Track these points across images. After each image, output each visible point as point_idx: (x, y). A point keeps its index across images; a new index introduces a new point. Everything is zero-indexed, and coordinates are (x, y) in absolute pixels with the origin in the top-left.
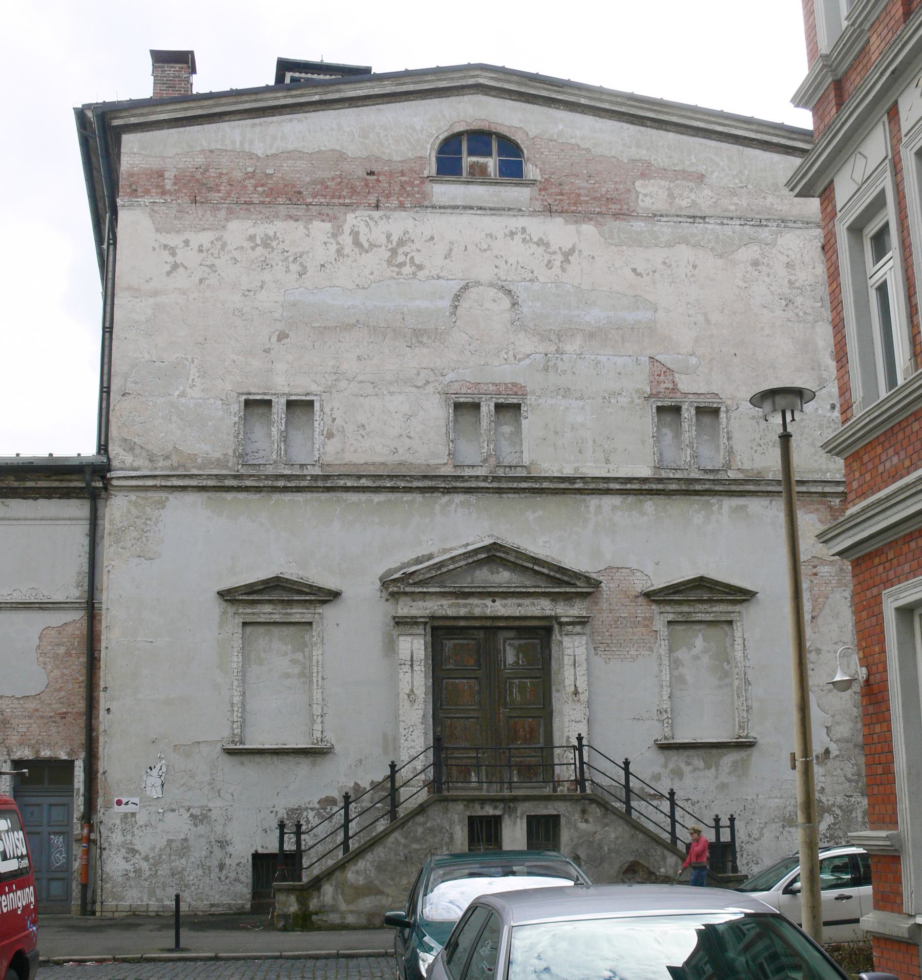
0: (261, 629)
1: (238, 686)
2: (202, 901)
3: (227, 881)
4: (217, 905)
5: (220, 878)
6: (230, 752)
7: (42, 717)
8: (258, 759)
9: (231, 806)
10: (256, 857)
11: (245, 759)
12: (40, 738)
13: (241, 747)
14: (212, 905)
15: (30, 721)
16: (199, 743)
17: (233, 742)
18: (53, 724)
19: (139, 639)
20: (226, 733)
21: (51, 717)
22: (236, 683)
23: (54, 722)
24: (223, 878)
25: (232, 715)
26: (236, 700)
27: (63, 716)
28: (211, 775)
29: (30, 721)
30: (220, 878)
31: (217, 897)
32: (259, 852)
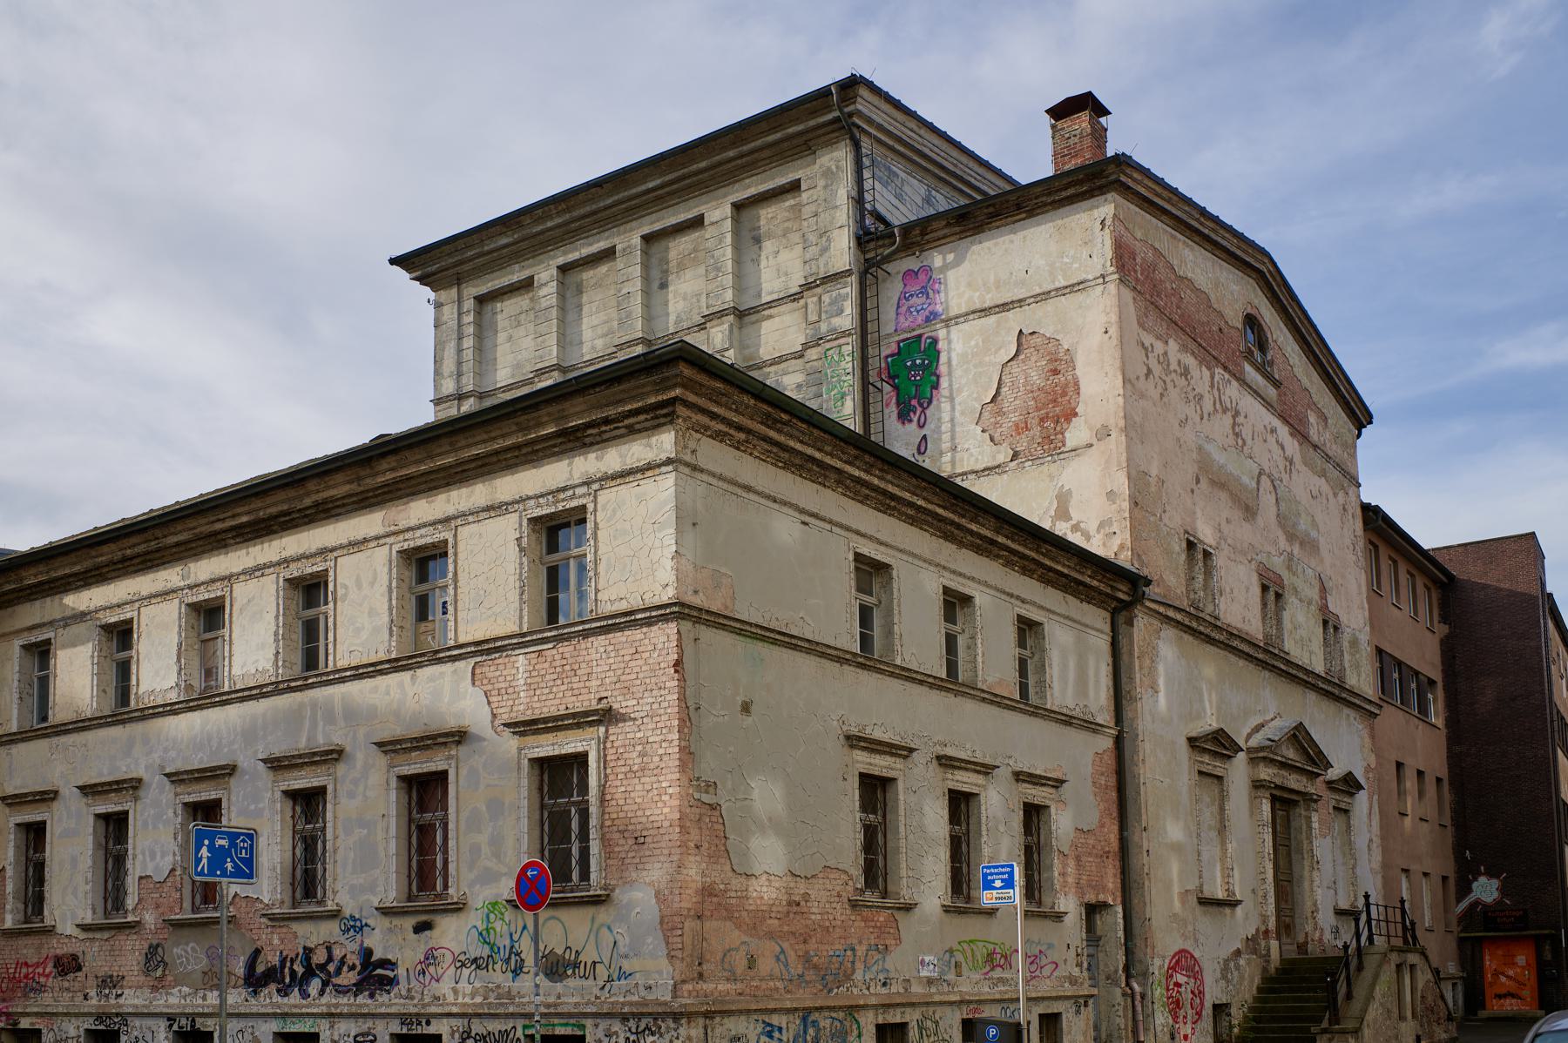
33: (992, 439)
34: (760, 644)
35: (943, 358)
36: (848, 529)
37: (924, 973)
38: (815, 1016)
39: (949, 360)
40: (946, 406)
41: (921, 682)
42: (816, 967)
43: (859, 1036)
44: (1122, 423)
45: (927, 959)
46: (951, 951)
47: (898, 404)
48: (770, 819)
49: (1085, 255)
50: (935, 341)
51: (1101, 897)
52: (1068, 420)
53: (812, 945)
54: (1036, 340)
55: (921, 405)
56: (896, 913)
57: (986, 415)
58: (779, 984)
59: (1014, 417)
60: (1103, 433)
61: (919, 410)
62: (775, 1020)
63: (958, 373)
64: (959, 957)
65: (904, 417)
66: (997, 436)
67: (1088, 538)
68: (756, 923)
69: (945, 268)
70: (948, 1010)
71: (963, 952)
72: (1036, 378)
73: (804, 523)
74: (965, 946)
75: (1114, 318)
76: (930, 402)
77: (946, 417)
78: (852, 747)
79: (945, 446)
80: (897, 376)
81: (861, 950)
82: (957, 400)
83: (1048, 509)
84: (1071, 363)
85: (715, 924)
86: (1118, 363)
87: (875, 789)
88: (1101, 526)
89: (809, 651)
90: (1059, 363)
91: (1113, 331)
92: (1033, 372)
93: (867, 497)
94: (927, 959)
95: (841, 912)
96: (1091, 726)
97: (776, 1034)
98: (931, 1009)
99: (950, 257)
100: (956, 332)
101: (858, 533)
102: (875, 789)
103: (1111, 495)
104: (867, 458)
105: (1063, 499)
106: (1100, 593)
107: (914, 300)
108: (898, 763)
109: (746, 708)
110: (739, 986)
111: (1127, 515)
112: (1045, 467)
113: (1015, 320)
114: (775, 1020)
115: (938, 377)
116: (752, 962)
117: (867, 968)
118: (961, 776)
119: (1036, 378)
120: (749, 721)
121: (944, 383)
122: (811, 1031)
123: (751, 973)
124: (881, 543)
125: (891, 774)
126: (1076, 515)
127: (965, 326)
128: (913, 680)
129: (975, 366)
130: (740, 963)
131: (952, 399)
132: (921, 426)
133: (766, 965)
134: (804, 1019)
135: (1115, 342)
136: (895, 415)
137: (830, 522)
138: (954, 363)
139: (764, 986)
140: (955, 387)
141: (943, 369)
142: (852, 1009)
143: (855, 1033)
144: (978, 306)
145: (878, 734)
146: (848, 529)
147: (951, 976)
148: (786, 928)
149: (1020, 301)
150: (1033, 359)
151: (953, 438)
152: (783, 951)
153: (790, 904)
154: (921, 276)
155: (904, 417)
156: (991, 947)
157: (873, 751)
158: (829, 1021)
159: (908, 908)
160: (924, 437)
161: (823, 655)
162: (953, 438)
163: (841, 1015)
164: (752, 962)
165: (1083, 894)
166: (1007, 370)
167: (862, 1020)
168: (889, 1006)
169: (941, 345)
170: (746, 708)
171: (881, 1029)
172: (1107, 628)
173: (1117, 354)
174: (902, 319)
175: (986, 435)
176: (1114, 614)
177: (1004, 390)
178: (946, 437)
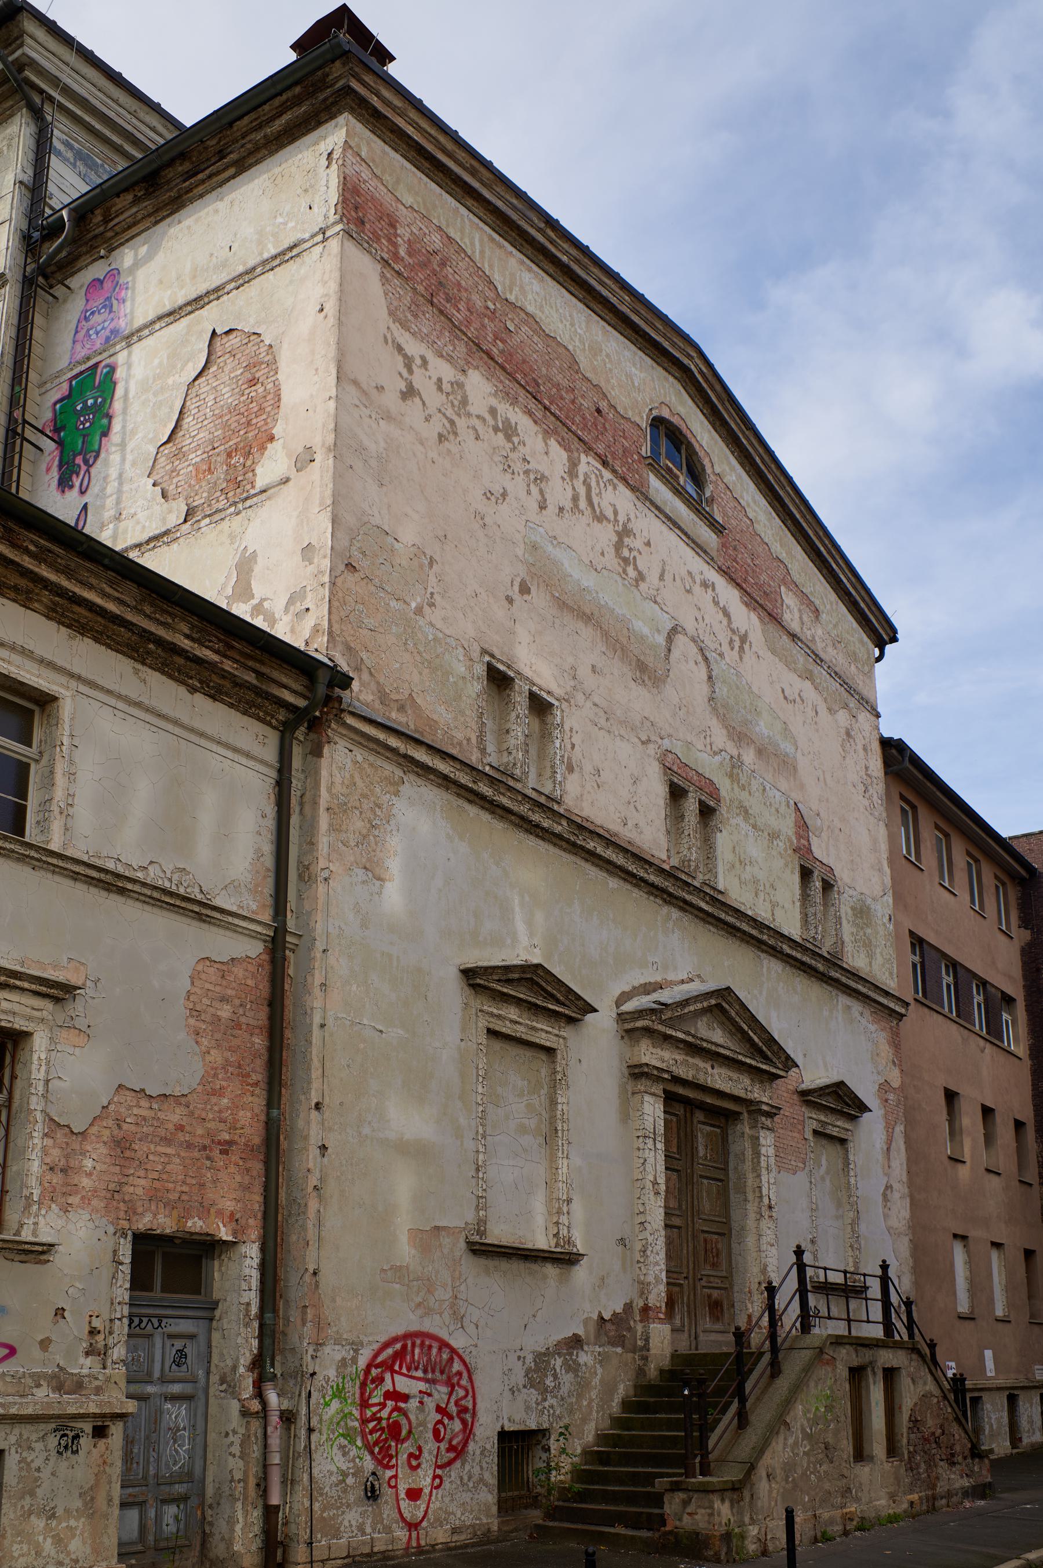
5: (461, 1478)
7: (189, 1146)
10: (504, 1436)
12: (185, 1188)
15: (169, 1151)
18: (208, 1163)
19: (365, 1022)
21: (205, 1148)
23: (208, 1158)
27: (226, 1147)
29: (169, 1151)
30: (461, 1478)
32: (506, 1429)
33: (164, 495)
35: (119, 392)
39: (126, 396)
40: (115, 458)
44: (330, 439)
47: (60, 466)
49: (304, 206)
50: (112, 369)
51: (195, 1224)
52: (263, 448)
54: (234, 340)
55: (86, 462)
57: (162, 460)
59: (195, 458)
60: (305, 459)
61: (84, 468)
63: (135, 407)
65: (64, 484)
66: (171, 489)
67: (273, 621)
69: (136, 265)
72: (228, 396)
75: (333, 286)
76: (97, 457)
77: (113, 473)
79: (108, 514)
80: (63, 428)
82: (129, 449)
83: (224, 586)
84: (273, 365)
86: (332, 352)
88: (291, 601)
90: (259, 369)
91: (331, 308)
92: (223, 389)
96: (201, 910)
99: (143, 250)
100: (139, 351)
103: (308, 552)
105: (245, 566)
106: (238, 684)
107: (97, 318)
111: (326, 579)
112: (225, 524)
113: (211, 317)
115: (110, 418)
119: (228, 396)
121: (117, 426)
126: (258, 590)
127: (149, 342)
129: (155, 395)
131: (123, 445)
132: (82, 493)
135: (331, 321)
136: (55, 482)
138: (131, 395)
140: (130, 426)
141: (117, 406)
144: (168, 307)
149: (217, 289)
150: (227, 369)
151: (118, 502)
154: (108, 285)
155: (64, 484)
160: (85, 507)
162: (118, 502)
166: (193, 392)
169: (120, 374)
172: (271, 754)
173: (333, 340)
174: (78, 347)
175: (158, 489)
176: (286, 732)
177: (188, 420)
178: (110, 502)
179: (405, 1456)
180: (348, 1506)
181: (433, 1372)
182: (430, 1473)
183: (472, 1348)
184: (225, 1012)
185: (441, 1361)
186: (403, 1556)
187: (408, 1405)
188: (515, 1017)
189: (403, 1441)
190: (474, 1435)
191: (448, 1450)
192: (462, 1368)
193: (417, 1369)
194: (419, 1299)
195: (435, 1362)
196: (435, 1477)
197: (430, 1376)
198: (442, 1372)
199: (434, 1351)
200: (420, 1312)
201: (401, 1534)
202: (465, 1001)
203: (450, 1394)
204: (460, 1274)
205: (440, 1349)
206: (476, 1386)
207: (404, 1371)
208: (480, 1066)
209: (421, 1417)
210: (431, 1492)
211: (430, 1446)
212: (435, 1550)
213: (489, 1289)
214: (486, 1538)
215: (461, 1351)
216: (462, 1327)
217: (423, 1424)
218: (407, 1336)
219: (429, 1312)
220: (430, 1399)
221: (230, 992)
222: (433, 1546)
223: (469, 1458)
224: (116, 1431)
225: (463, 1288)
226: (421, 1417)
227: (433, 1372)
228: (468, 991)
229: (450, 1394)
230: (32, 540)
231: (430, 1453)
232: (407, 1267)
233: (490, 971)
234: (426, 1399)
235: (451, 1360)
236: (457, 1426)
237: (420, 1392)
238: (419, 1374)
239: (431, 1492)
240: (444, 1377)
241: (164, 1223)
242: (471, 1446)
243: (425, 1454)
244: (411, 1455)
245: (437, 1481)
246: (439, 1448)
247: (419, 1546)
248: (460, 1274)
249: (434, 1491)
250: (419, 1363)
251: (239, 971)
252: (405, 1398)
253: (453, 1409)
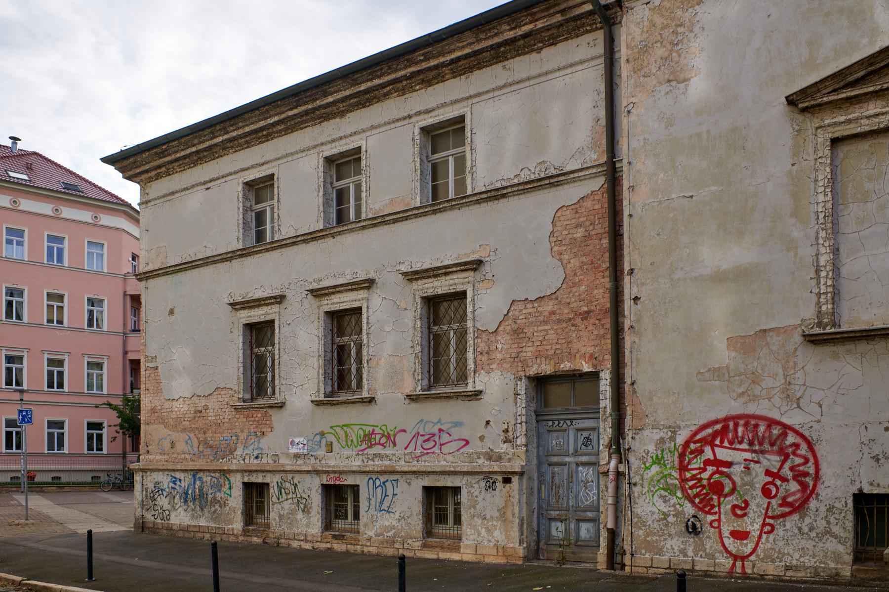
0: (864, 146)
1: (826, 238)
2: (773, 561)
3: (813, 534)
4: (797, 569)
5: (800, 529)
6: (813, 340)
7: (559, 321)
8: (863, 347)
9: (819, 421)
10: (860, 499)
11: (840, 349)
12: (558, 346)
13: (833, 330)
14: (788, 568)
15: (546, 327)
16: (765, 331)
17: (819, 324)
18: (573, 328)
19: (674, 196)
20: (809, 313)
21: (570, 320)
22: (822, 234)
23: (573, 325)
24: (806, 529)
25: (819, 283)
26: (823, 260)
27: (585, 316)
28: (785, 377)
29: (546, 327)
30: (800, 529)
31: (796, 556)
32: (865, 491)
34: (179, 274)
36: (236, 173)
37: (294, 450)
38: (200, 475)
41: (294, 244)
42: (211, 447)
43: (230, 488)
45: (296, 440)
46: (322, 434)
48: (184, 368)
53: (209, 435)
56: (269, 410)
58: (187, 456)
62: (178, 475)
64: (331, 438)
68: (177, 425)
70: (307, 478)
71: (336, 434)
73: (208, 189)
74: (338, 429)
78: (237, 310)
81: (242, 436)
85: (155, 426)
87: (259, 334)
89: (207, 264)
93: (246, 142)
94: (296, 440)
95: (228, 413)
97: (178, 483)
98: (290, 476)
101: (243, 170)
102: (259, 334)
104: (218, 127)
108: (275, 308)
109: (171, 312)
110: (166, 457)
114: (178, 475)
116: (173, 445)
117: (246, 447)
118: (335, 298)
120: (173, 318)
122: (198, 483)
123: (173, 450)
124: (263, 164)
125: (269, 318)
128: (286, 245)
130: (167, 445)
133: (181, 446)
134: (194, 476)
137: (223, 177)
139: (179, 457)
142: (224, 473)
143: (227, 486)
145: (259, 294)
146: (236, 173)
147: (321, 452)
148: (193, 426)
152: (190, 438)
153: (195, 412)
156: (368, 429)
157: (250, 308)
158: (209, 478)
159: (281, 406)
161: (215, 262)
163: (217, 475)
164: (173, 445)
165: (525, 365)
167: (232, 479)
168: (251, 471)
170: (171, 312)
171: (247, 486)
179: (730, 506)
180: (670, 535)
181: (761, 444)
182: (760, 521)
183: (815, 425)
184: (579, 233)
185: (770, 436)
186: (726, 577)
187: (732, 469)
188: (878, 110)
189: (726, 496)
190: (818, 495)
191: (781, 505)
192: (798, 440)
193: (740, 443)
194: (742, 390)
195: (763, 436)
196: (764, 525)
197: (757, 448)
198: (772, 444)
199: (762, 429)
200: (742, 400)
201: (725, 562)
202: (797, 128)
203: (783, 462)
204: (795, 363)
205: (769, 427)
206: (819, 455)
207: (726, 444)
208: (821, 177)
209: (747, 479)
210: (760, 537)
211: (758, 502)
212: (764, 579)
213: (822, 371)
214: (834, 580)
215: (797, 427)
216: (799, 407)
217: (751, 484)
218: (726, 419)
219: (754, 398)
220: (758, 465)
221: (582, 220)
222: (762, 575)
223: (811, 513)
224: (515, 480)
225: (798, 375)
226: (747, 479)
227: (761, 444)
228: (800, 117)
229: (783, 462)
230: (419, 55)
231: (758, 505)
232: (727, 367)
233: (809, 91)
234: (752, 465)
235: (784, 435)
236: (794, 486)
237: (745, 460)
238: (745, 446)
239: (760, 537)
240: (775, 448)
241: (546, 368)
242: (813, 504)
243: (753, 506)
244: (735, 507)
245: (768, 528)
246: (769, 503)
247: (744, 572)
248: (795, 363)
249: (764, 536)
250: (743, 438)
251: (588, 204)
252: (729, 464)
253: (786, 472)
